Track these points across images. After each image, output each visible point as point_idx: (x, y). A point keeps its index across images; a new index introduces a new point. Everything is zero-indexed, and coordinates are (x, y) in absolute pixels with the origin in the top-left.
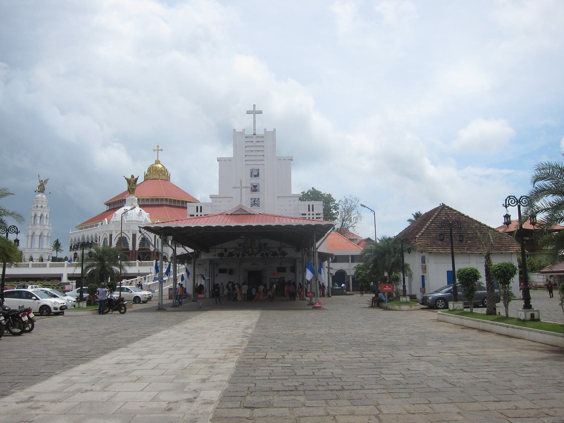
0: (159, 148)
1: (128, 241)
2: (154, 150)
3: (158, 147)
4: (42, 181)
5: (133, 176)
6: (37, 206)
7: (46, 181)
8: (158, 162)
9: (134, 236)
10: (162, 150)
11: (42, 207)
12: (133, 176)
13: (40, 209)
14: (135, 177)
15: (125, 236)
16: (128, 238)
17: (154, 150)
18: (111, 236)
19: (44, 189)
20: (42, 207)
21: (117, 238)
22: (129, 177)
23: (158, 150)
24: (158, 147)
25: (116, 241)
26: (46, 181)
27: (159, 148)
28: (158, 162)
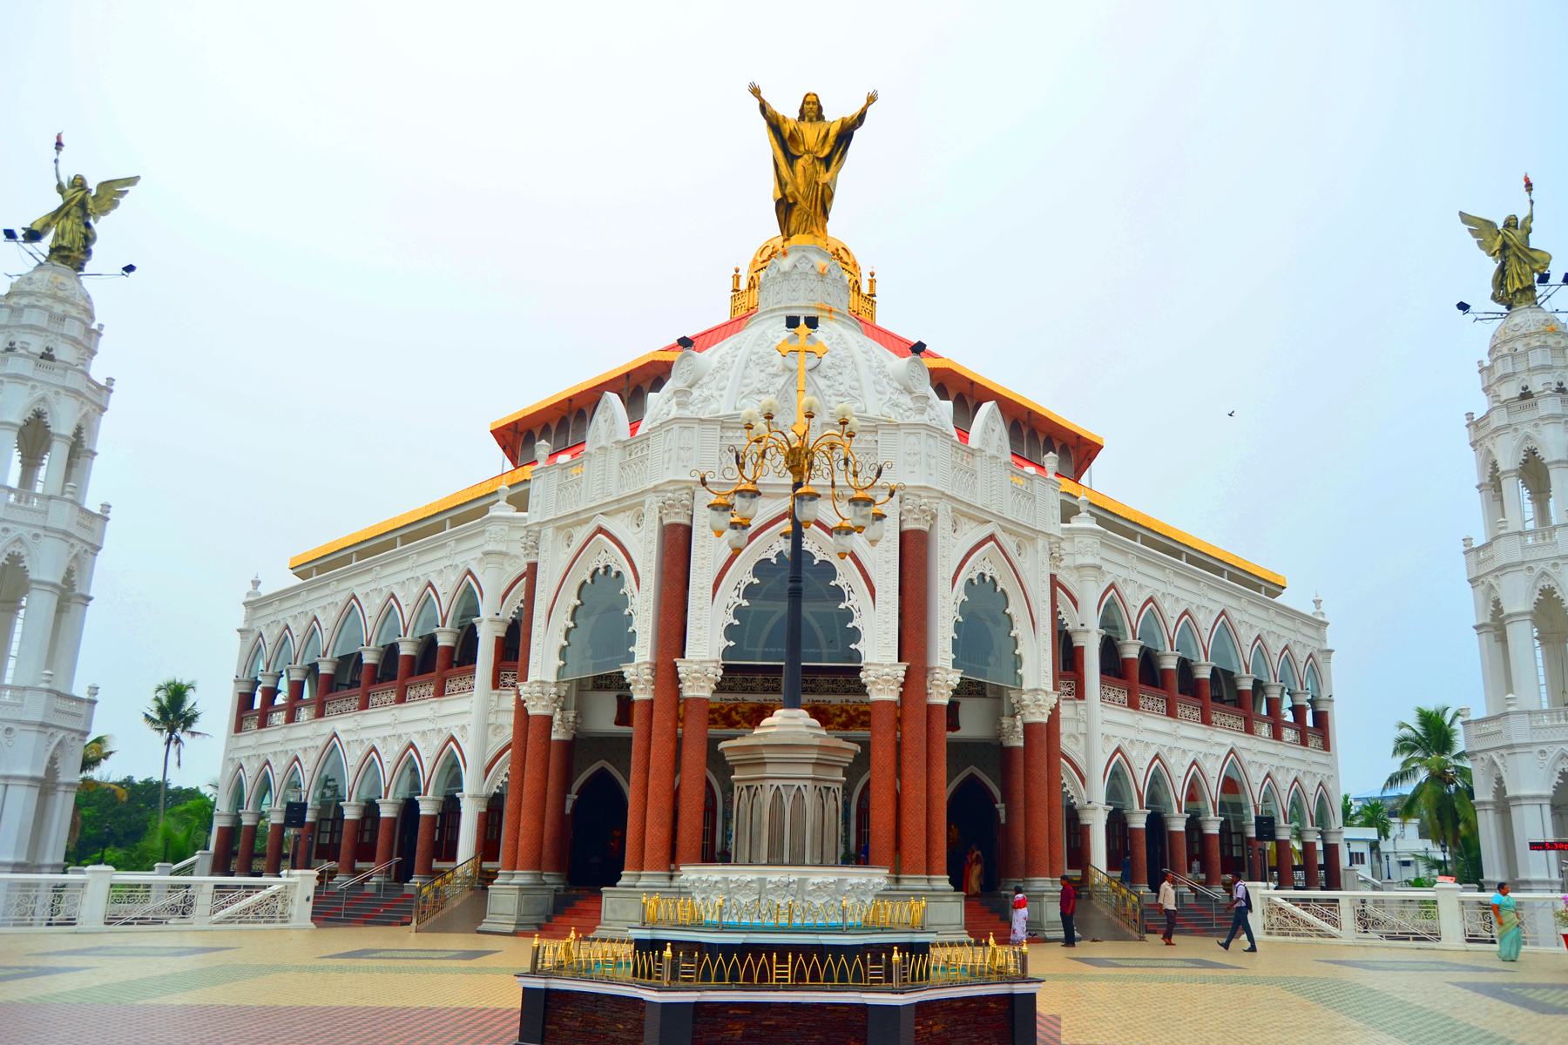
1: (857, 599)
4: (79, 183)
5: (812, 110)
7: (112, 192)
9: (914, 552)
11: (47, 356)
12: (812, 110)
14: (836, 112)
18: (677, 546)
19: (88, 239)
20: (47, 356)
21: (742, 573)
25: (731, 596)
26: (112, 192)
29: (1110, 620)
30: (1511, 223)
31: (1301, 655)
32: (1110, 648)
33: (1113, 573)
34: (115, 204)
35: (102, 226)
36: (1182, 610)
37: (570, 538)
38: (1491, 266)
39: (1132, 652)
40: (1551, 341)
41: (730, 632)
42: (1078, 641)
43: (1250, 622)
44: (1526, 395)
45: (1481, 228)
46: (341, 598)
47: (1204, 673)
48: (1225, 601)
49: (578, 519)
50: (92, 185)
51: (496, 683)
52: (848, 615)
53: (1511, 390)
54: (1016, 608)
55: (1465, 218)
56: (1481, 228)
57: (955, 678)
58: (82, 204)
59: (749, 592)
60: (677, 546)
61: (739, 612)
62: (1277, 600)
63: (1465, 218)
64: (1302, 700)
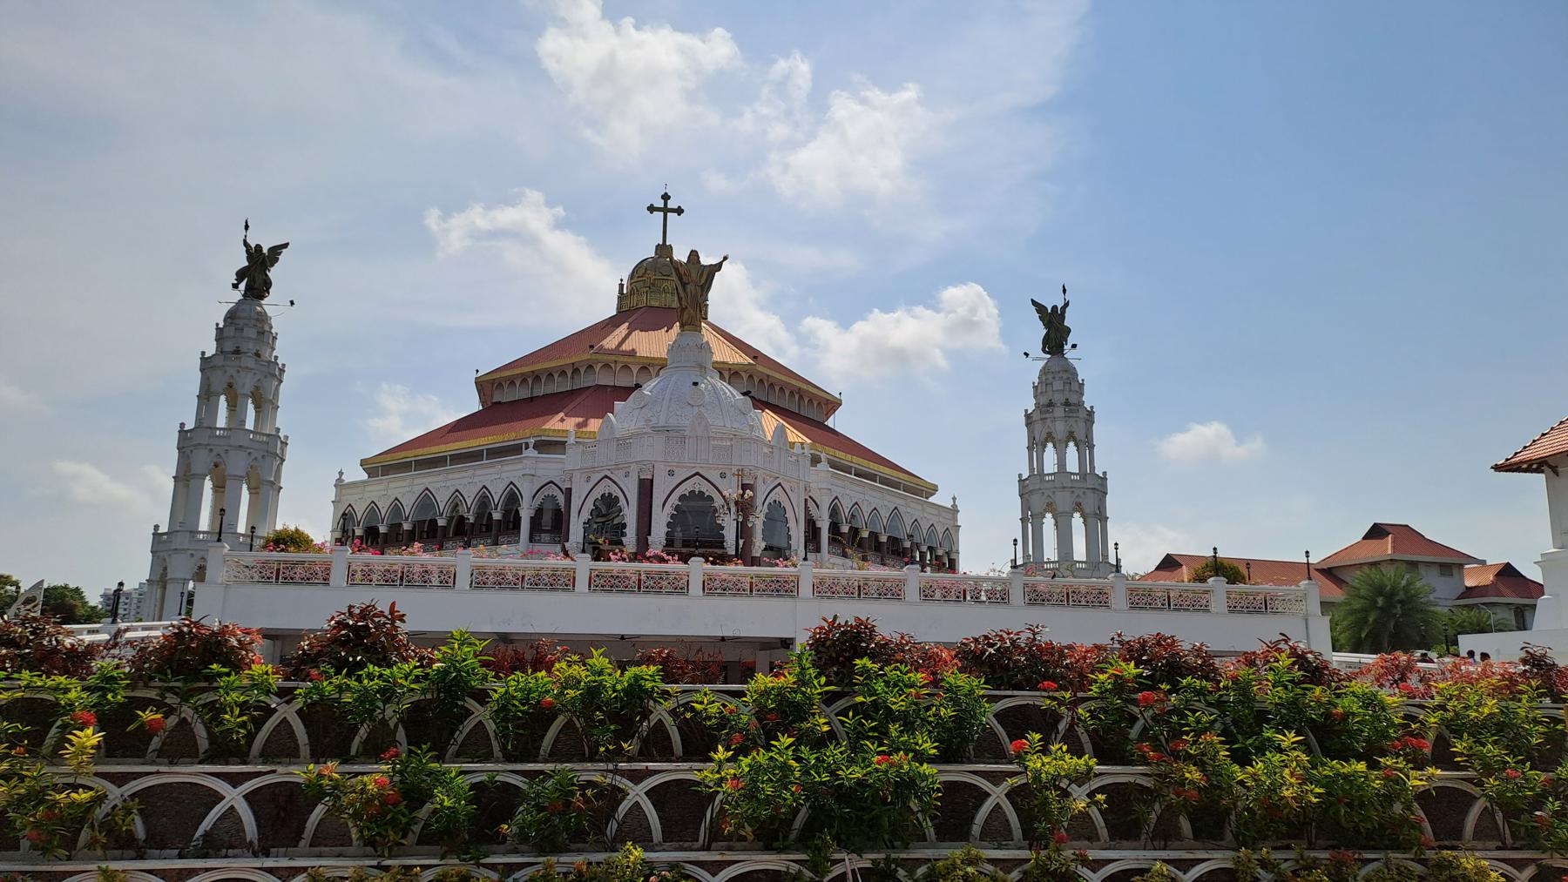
0: (671, 204)
2: (652, 209)
3: (666, 197)
4: (259, 247)
6: (237, 352)
7: (276, 251)
8: (664, 249)
10: (679, 211)
13: (249, 362)
15: (708, 490)
17: (652, 209)
18: (646, 488)
19: (268, 284)
23: (665, 210)
24: (666, 197)
25: (669, 509)
26: (276, 251)
27: (671, 205)
28: (664, 249)
29: (834, 512)
30: (1055, 307)
31: (940, 530)
32: (834, 527)
33: (838, 491)
34: (277, 260)
35: (274, 273)
39: (845, 529)
40: (1065, 376)
42: (819, 524)
44: (1051, 404)
46: (418, 490)
47: (884, 539)
48: (898, 502)
49: (593, 469)
50: (265, 251)
53: (1044, 400)
54: (790, 515)
55: (1034, 302)
57: (763, 545)
58: (264, 262)
60: (646, 488)
61: (672, 516)
62: (931, 500)
63: (1034, 302)
64: (940, 552)
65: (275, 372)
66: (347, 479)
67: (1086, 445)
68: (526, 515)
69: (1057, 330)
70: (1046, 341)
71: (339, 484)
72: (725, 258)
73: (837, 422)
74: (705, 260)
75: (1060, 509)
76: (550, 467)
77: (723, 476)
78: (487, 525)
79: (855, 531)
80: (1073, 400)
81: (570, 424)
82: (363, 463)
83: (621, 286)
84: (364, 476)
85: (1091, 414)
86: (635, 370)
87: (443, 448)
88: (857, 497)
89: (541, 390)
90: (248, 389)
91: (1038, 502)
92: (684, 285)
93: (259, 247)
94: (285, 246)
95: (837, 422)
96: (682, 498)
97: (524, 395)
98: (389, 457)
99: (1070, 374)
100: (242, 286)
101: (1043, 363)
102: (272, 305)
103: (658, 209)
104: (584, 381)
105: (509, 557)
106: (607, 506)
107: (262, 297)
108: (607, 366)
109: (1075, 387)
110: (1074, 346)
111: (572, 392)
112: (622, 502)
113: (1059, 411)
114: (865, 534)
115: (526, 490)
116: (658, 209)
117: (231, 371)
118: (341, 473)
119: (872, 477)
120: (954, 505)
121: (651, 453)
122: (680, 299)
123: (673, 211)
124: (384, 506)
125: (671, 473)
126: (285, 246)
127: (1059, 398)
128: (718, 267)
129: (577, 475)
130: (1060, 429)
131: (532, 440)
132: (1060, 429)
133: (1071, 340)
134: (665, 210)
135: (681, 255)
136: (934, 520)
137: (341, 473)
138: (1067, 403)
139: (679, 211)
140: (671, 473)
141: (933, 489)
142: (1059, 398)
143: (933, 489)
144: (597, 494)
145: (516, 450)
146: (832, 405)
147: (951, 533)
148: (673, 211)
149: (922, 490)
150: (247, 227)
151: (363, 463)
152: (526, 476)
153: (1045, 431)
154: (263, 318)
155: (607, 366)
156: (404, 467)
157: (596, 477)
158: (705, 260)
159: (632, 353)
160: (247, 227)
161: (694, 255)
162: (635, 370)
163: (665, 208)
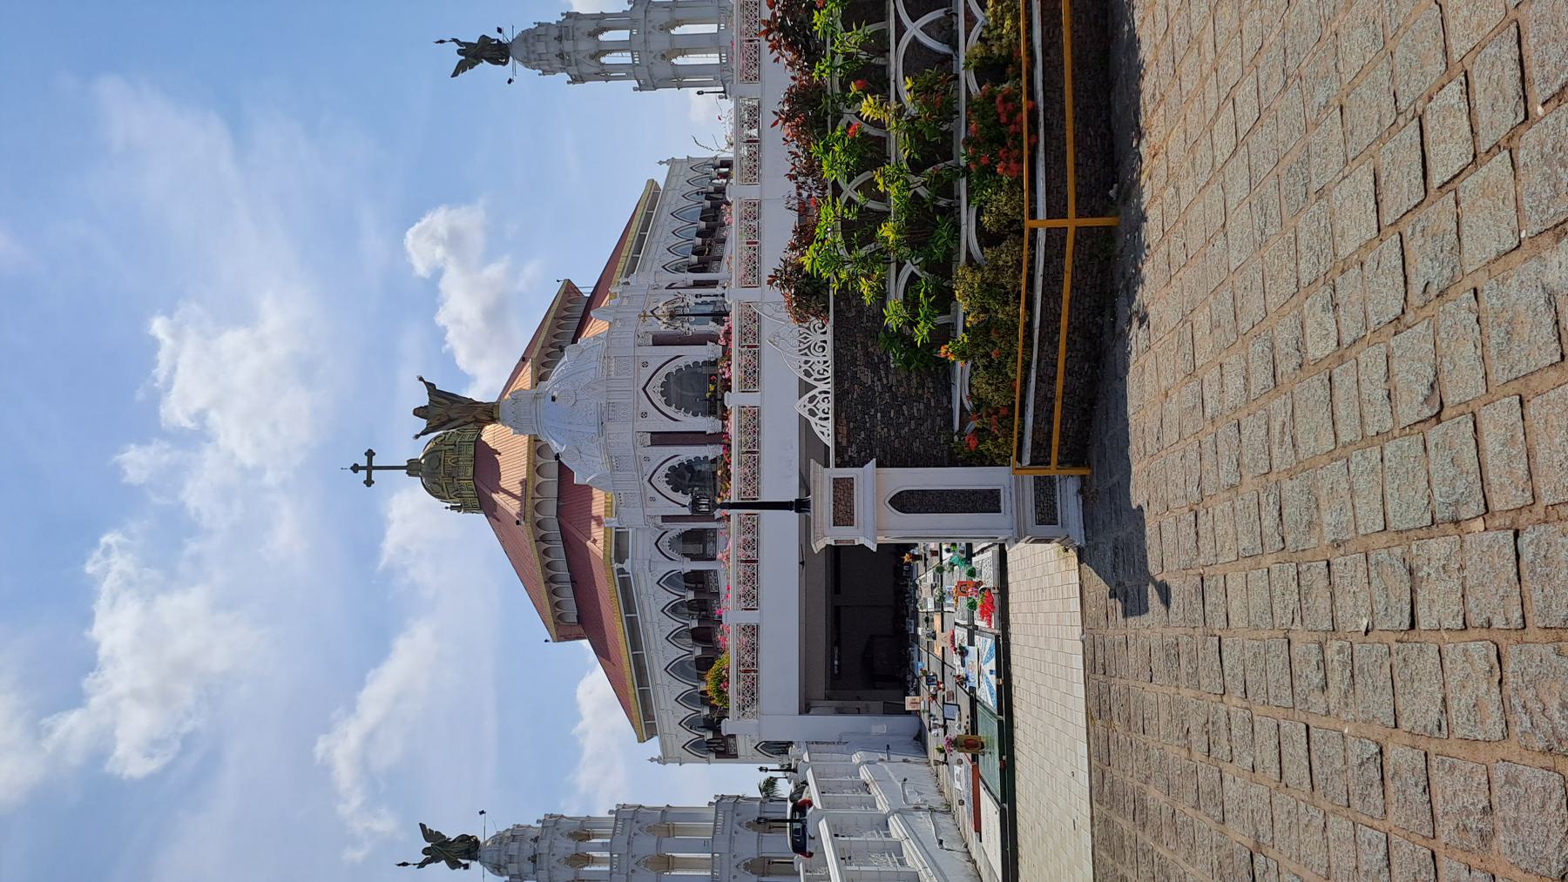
1: (681, 363)
2: (369, 482)
3: (355, 468)
4: (425, 851)
6: (533, 859)
7: (428, 834)
8: (412, 468)
9: (659, 341)
10: (370, 454)
13: (543, 846)
16: (671, 368)
17: (369, 482)
18: (660, 438)
19: (464, 838)
22: (422, 424)
23: (370, 468)
24: (355, 468)
25: (680, 415)
26: (428, 834)
28: (412, 468)
30: (459, 52)
31: (692, 174)
33: (657, 266)
35: (451, 834)
36: (671, 237)
37: (652, 499)
38: (485, 65)
39: (695, 259)
41: (695, 415)
43: (674, 201)
44: (561, 55)
45: (461, 68)
47: (703, 224)
48: (666, 212)
49: (643, 495)
51: (713, 559)
52: (688, 366)
53: (557, 63)
55: (455, 74)
56: (461, 68)
59: (678, 408)
60: (660, 438)
63: (455, 74)
64: (715, 174)
65: (552, 823)
66: (658, 753)
67: (601, 22)
68: (689, 566)
69: (483, 49)
70: (494, 61)
71: (663, 760)
72: (421, 379)
73: (586, 286)
74: (425, 401)
75: (667, 46)
76: (641, 545)
77: (645, 364)
78: (699, 601)
79: (697, 252)
80: (555, 33)
81: (597, 532)
82: (641, 740)
83: (452, 508)
84: (656, 739)
85: (569, 15)
86: (540, 480)
87: (625, 659)
88: (662, 249)
89: (563, 573)
90: (572, 844)
91: (661, 70)
92: (450, 420)
93: (425, 851)
94: (423, 826)
95: (586, 286)
96: (668, 403)
97: (572, 597)
98: (635, 714)
99: (526, 36)
100: (464, 862)
101: (519, 66)
102: (484, 832)
103: (369, 475)
104: (554, 529)
105: (728, 575)
106: (682, 477)
107: (477, 842)
108: (537, 508)
109: (542, 31)
110: (500, 30)
111: (565, 541)
112: (674, 462)
113: (568, 46)
114: (699, 241)
115: (664, 567)
116: (369, 475)
117: (553, 860)
118: (652, 760)
119: (641, 239)
120: (667, 162)
121: (626, 435)
122: (466, 423)
123: (370, 460)
124: (685, 712)
125: (644, 415)
126: (423, 826)
127: (555, 48)
128: (431, 386)
129: (648, 511)
130: (586, 46)
131: (616, 566)
132: (586, 46)
133: (494, 35)
134: (370, 468)
135: (422, 424)
136: (683, 180)
137: (652, 760)
138: (559, 39)
139: (370, 454)
140: (644, 415)
141: (652, 183)
142: (555, 48)
143: (652, 183)
144: (667, 489)
145: (625, 584)
146: (569, 289)
147: (694, 165)
148: (370, 460)
149: (653, 196)
150: (405, 864)
151: (641, 740)
152: (651, 568)
153: (588, 60)
154: (499, 839)
155: (537, 508)
156: (644, 697)
157: (652, 492)
158: (425, 401)
159: (524, 483)
160: (405, 864)
161: (419, 412)
162: (540, 480)
163: (368, 468)
